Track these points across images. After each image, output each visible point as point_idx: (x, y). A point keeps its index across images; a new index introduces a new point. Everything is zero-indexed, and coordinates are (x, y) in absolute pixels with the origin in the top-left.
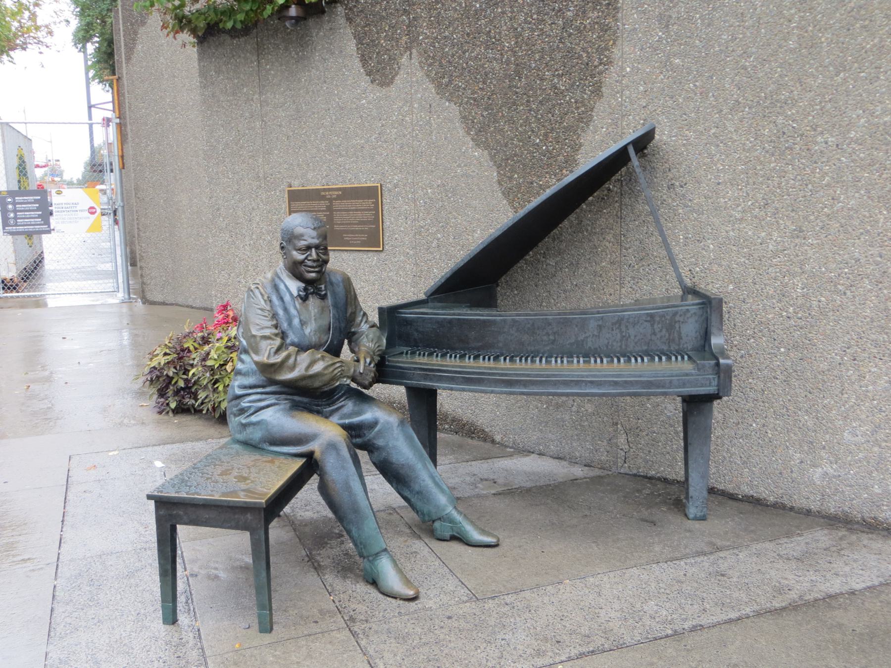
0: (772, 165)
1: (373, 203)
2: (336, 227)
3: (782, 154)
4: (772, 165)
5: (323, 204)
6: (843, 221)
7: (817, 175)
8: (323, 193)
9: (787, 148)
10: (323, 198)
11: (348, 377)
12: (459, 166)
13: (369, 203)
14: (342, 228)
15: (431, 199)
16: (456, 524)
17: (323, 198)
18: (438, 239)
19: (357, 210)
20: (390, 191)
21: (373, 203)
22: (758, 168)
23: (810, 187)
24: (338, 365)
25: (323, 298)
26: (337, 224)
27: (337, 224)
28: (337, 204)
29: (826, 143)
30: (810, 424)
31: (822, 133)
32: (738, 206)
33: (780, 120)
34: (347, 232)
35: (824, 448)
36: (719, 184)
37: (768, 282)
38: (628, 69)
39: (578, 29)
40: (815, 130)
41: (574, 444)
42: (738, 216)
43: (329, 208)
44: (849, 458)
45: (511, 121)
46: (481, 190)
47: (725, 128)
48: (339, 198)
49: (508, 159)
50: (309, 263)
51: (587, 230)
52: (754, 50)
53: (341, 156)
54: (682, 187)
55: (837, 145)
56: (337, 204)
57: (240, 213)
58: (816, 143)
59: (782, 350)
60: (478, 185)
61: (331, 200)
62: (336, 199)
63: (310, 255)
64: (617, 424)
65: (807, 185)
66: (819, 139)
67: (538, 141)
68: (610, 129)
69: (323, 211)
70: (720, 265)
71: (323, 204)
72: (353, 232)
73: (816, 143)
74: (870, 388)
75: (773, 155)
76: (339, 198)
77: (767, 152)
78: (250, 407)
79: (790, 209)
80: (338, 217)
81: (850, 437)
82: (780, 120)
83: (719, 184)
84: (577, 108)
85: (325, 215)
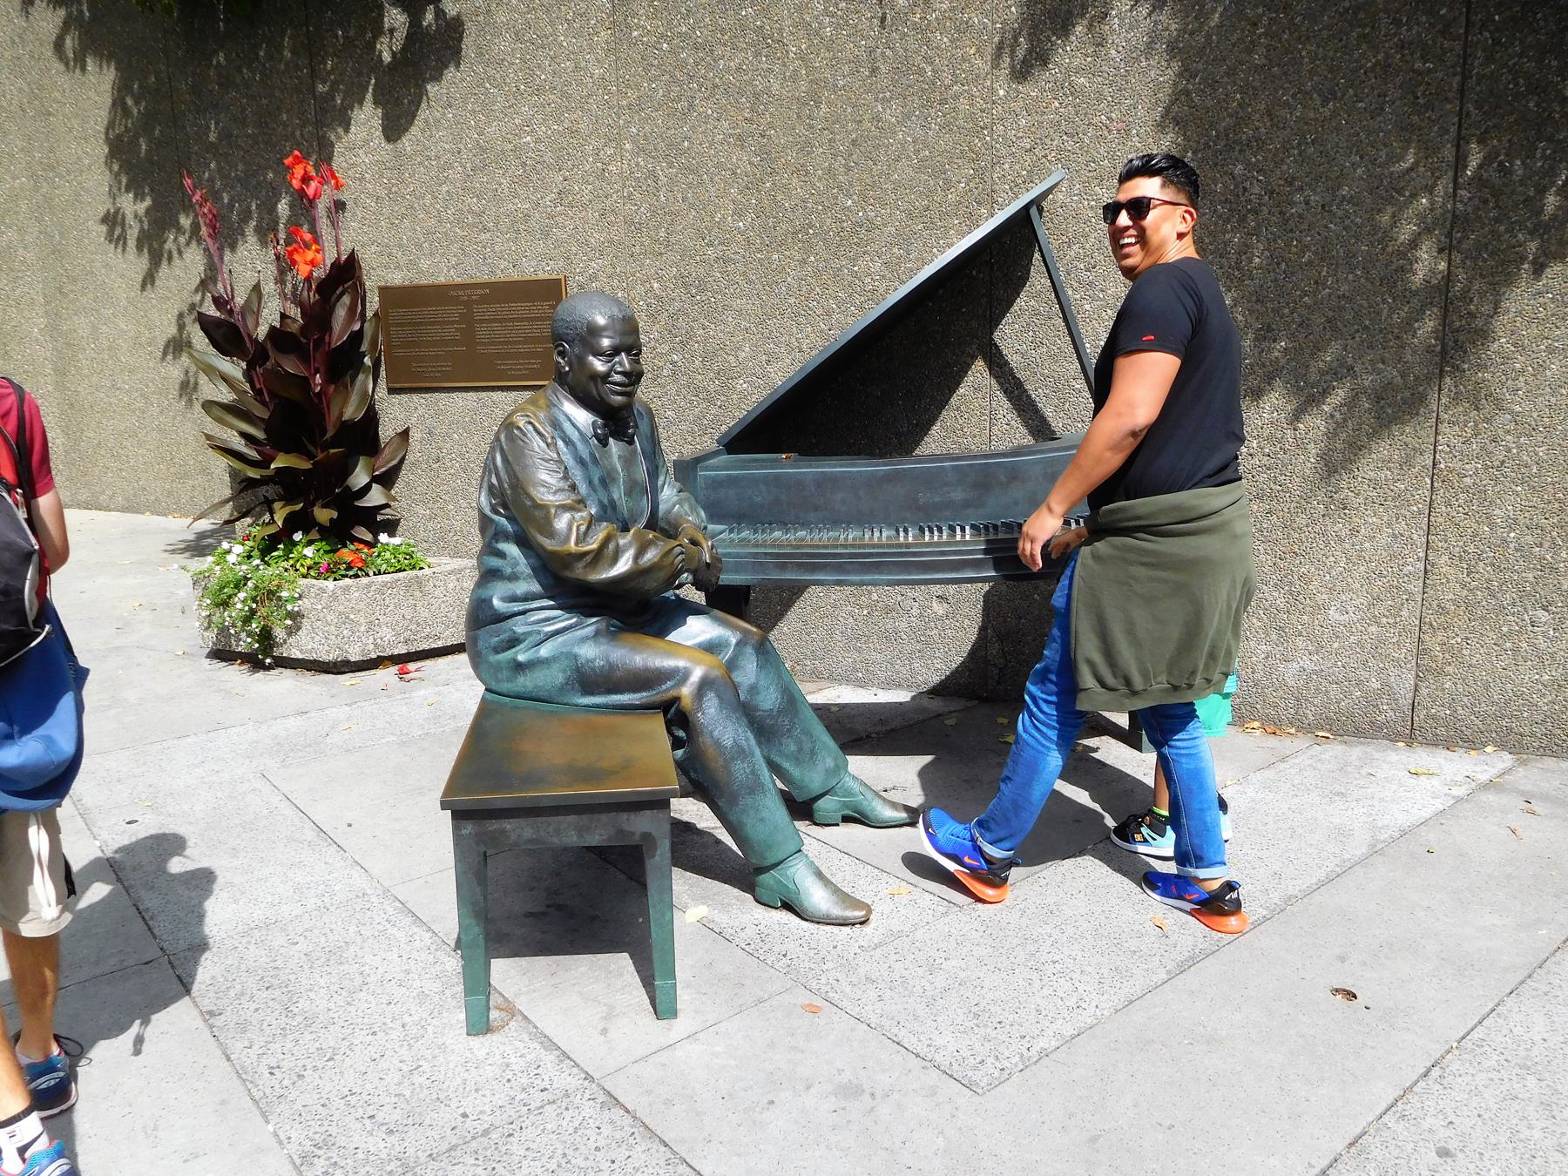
3: (1243, 219)
5: (454, 312)
6: (1330, 314)
12: (710, 244)
14: (492, 349)
15: (659, 298)
16: (854, 795)
17: (456, 301)
18: (673, 363)
19: (519, 320)
23: (1283, 266)
24: (678, 549)
29: (1307, 203)
31: (1301, 189)
38: (1002, 92)
39: (915, 27)
40: (1291, 184)
44: (1336, 645)
45: (802, 171)
46: (751, 282)
48: (484, 299)
50: (617, 378)
52: (1200, 66)
53: (485, 229)
56: (481, 311)
58: (1292, 204)
61: (468, 304)
62: (478, 302)
65: (1278, 264)
66: (1298, 197)
69: (453, 323)
71: (454, 312)
72: (518, 356)
73: (1292, 204)
74: (1367, 545)
75: (1228, 221)
77: (1220, 217)
78: (529, 633)
80: (482, 332)
81: (1337, 616)
82: (1239, 169)
84: (917, 152)
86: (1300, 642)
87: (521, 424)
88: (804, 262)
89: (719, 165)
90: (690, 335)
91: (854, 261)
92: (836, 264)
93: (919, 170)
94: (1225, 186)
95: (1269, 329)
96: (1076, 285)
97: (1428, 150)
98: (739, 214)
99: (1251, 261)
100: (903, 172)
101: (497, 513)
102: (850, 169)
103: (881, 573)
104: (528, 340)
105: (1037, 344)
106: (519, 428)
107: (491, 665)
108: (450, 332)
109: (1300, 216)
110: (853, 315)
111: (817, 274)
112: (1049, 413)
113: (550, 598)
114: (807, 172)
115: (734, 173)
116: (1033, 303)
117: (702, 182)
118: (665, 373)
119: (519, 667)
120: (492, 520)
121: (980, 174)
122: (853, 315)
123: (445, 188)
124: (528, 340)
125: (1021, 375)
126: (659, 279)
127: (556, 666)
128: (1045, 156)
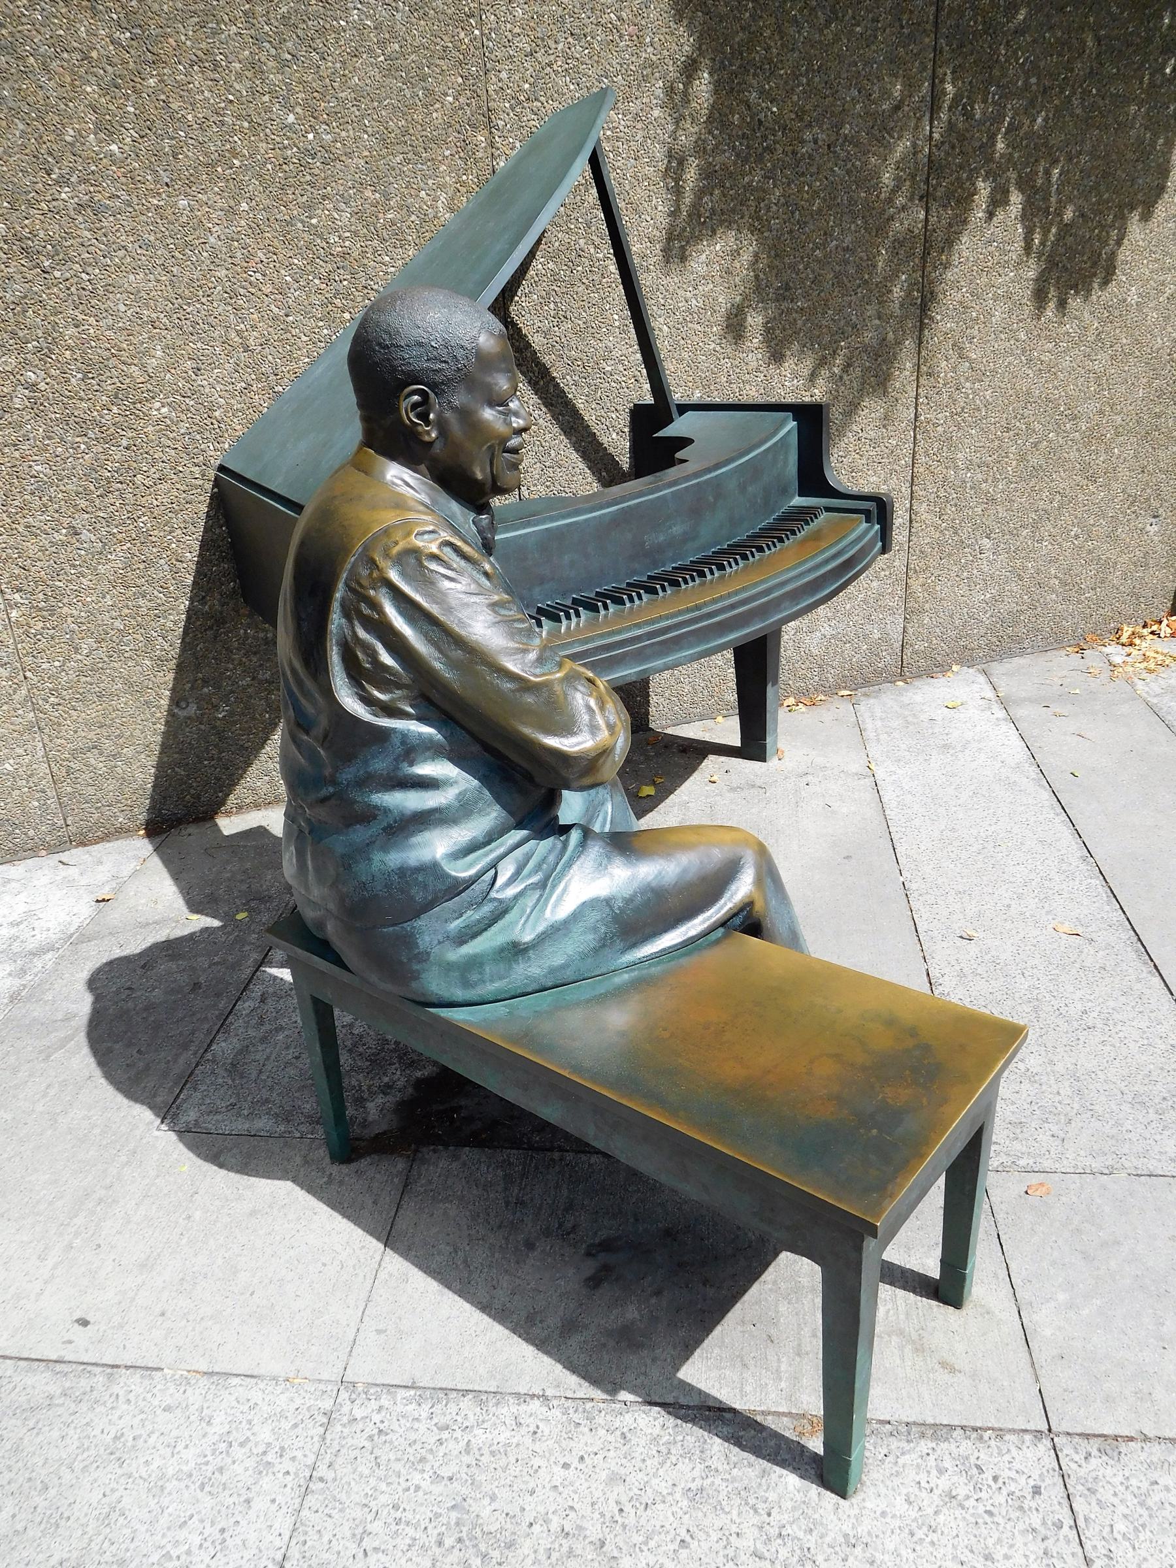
0: (746, 179)
4: (746, 179)
6: (838, 268)
7: (806, 196)
9: (765, 149)
12: (63, 181)
18: (33, 387)
22: (728, 185)
29: (816, 141)
40: (801, 120)
46: (149, 245)
49: (212, 165)
55: (829, 146)
60: (132, 232)
65: (793, 213)
67: (291, 118)
73: (802, 142)
79: (773, 253)
84: (382, 44)
87: (434, 548)
88: (231, 212)
89: (57, 43)
90: (52, 338)
91: (309, 207)
93: (390, 70)
94: (742, 119)
95: (787, 288)
97: (911, 85)
98: (107, 129)
99: (768, 209)
100: (366, 71)
101: (390, 711)
102: (285, 64)
103: (681, 649)
106: (434, 557)
107: (449, 967)
109: (810, 157)
110: (319, 291)
111: (256, 230)
112: (580, 404)
113: (519, 826)
114: (216, 66)
116: (551, 265)
118: (17, 403)
119: (516, 951)
120: (383, 735)
121: (472, 88)
122: (319, 291)
125: (547, 360)
127: (577, 929)
128: (550, 65)
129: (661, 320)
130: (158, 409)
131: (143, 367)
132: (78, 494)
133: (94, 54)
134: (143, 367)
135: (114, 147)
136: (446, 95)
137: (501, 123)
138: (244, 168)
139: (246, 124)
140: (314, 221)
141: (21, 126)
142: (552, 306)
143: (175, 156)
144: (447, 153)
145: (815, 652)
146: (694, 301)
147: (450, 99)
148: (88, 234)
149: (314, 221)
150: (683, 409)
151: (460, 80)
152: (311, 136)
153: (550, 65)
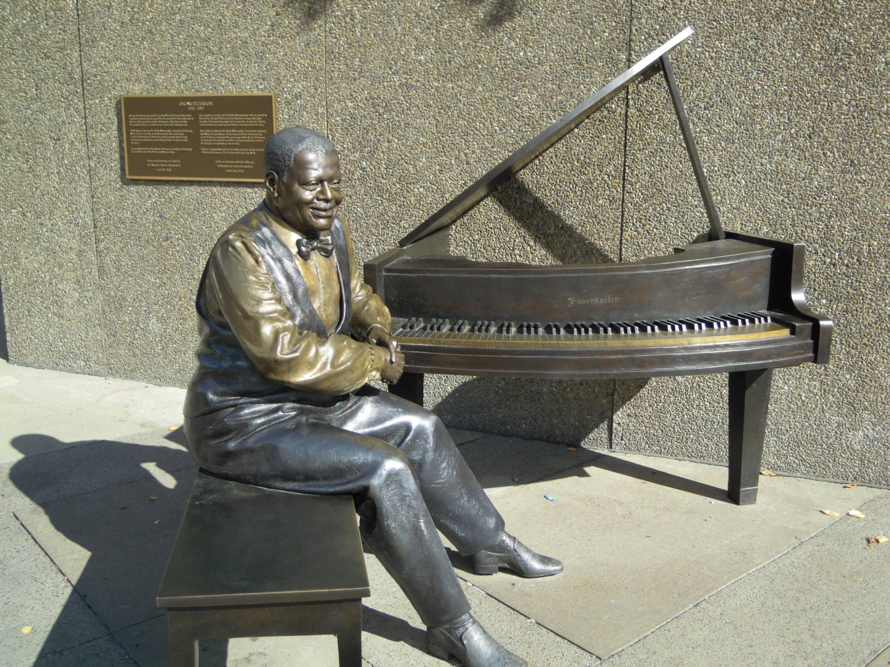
1: (263, 118)
2: (204, 151)
5: (184, 119)
8: (182, 104)
10: (185, 110)
11: (377, 369)
13: (258, 119)
14: (213, 151)
16: (509, 551)
17: (185, 110)
18: (363, 169)
20: (288, 103)
21: (263, 118)
25: (328, 254)
26: (205, 146)
27: (205, 146)
28: (205, 119)
30: (852, 384)
32: (776, 134)
33: (834, 33)
34: (223, 157)
35: (866, 409)
36: (756, 107)
37: (810, 223)
41: (554, 421)
42: (778, 145)
43: (194, 125)
46: (429, 106)
47: (765, 39)
48: (207, 110)
50: (323, 205)
51: (578, 160)
54: (705, 109)
56: (205, 119)
57: (42, 129)
59: (824, 301)
63: (323, 192)
64: (613, 394)
68: (614, 35)
69: (184, 128)
70: (753, 205)
71: (184, 119)
73: (875, 62)
75: (821, 75)
76: (207, 110)
83: (756, 107)
85: (186, 134)
86: (866, 415)
92: (501, 94)
96: (696, 120)
98: (420, 49)
99: (840, 107)
104: (244, 145)
105: (663, 167)
108: (179, 136)
115: (417, 15)
117: (391, 23)
123: (178, 17)
124: (244, 145)
126: (353, 99)
129: (740, 176)
130: (418, 189)
131: (415, 166)
132: (373, 225)
133: (421, 14)
134: (415, 166)
135: (422, 58)
136: (604, 32)
137: (637, 48)
138: (483, 69)
139: (488, 47)
140: (516, 98)
141: (383, 47)
142: (658, 158)
143: (450, 61)
144: (600, 64)
145: (858, 447)
146: (769, 166)
147: (607, 34)
148: (402, 98)
149: (516, 98)
150: (730, 236)
151: (614, 24)
152: (521, 54)
153: (675, 14)
